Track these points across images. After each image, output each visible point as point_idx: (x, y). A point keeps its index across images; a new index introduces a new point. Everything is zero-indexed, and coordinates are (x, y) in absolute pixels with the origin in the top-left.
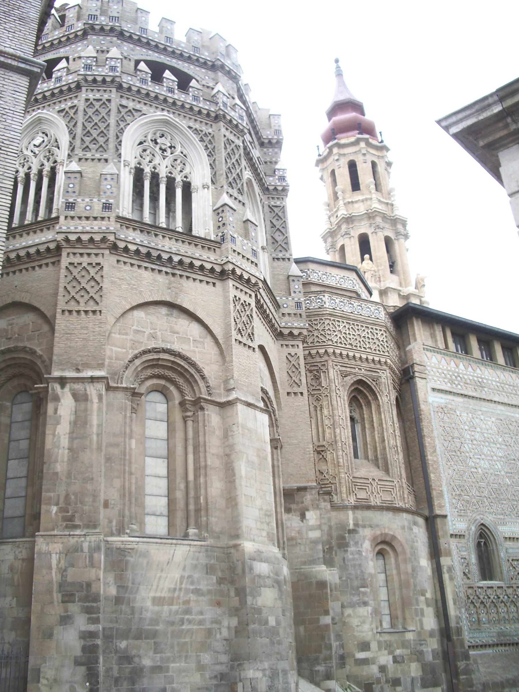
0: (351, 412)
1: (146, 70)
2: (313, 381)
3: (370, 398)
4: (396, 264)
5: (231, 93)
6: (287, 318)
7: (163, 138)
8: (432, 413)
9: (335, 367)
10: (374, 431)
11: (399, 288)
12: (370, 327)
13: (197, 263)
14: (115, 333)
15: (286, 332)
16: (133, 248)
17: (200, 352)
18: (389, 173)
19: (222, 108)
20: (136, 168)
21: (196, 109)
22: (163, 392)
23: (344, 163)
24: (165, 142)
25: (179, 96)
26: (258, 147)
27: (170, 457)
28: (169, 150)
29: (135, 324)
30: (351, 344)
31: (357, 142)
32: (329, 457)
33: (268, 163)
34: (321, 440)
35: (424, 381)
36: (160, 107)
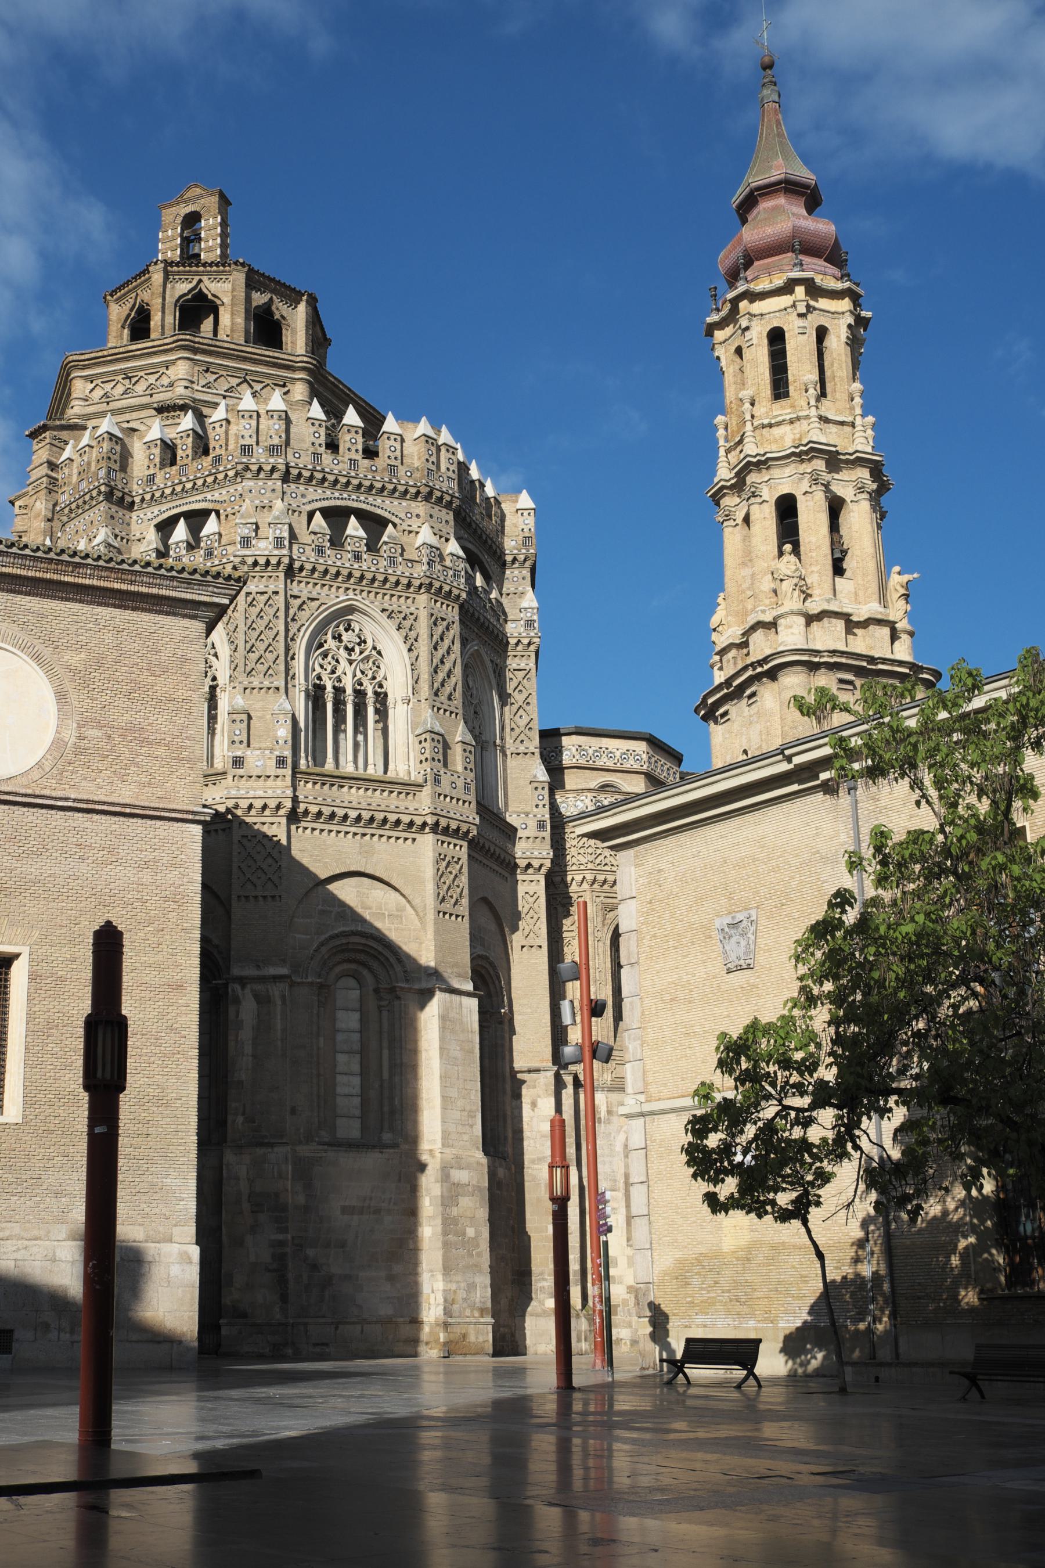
17: (396, 929)
22: (356, 976)
23: (758, 334)
25: (367, 562)
27: (363, 1052)
31: (787, 288)
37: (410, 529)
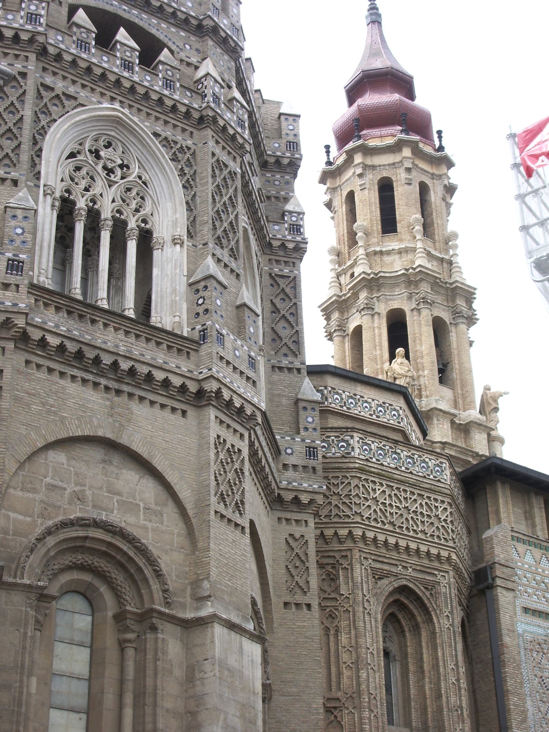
0: (384, 642)
1: (87, 26)
2: (325, 584)
3: (419, 619)
4: (449, 367)
5: (226, 77)
6: (290, 473)
7: (110, 149)
8: (522, 652)
9: (364, 562)
10: (423, 678)
11: (453, 411)
12: (426, 495)
13: (159, 376)
14: (15, 489)
15: (288, 496)
16: (53, 341)
17: (154, 530)
18: (449, 206)
19: (212, 105)
21: (169, 103)
26: (258, 169)
28: (119, 172)
29: (50, 474)
30: (392, 523)
31: (396, 148)
32: (346, 720)
33: (273, 199)
34: (334, 688)
35: (510, 595)
36: (109, 94)
37: (189, 60)
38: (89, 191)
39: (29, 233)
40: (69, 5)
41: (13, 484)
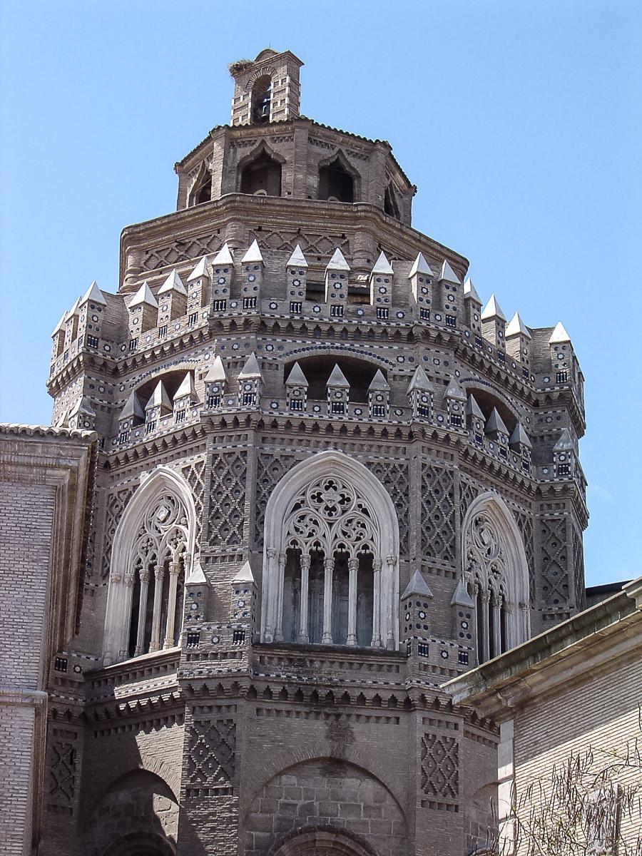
1: (299, 382)
13: (370, 695)
17: (373, 823)
20: (289, 551)
24: (331, 497)
37: (401, 373)
38: (313, 535)
39: (249, 604)
40: (285, 365)
41: (253, 809)
